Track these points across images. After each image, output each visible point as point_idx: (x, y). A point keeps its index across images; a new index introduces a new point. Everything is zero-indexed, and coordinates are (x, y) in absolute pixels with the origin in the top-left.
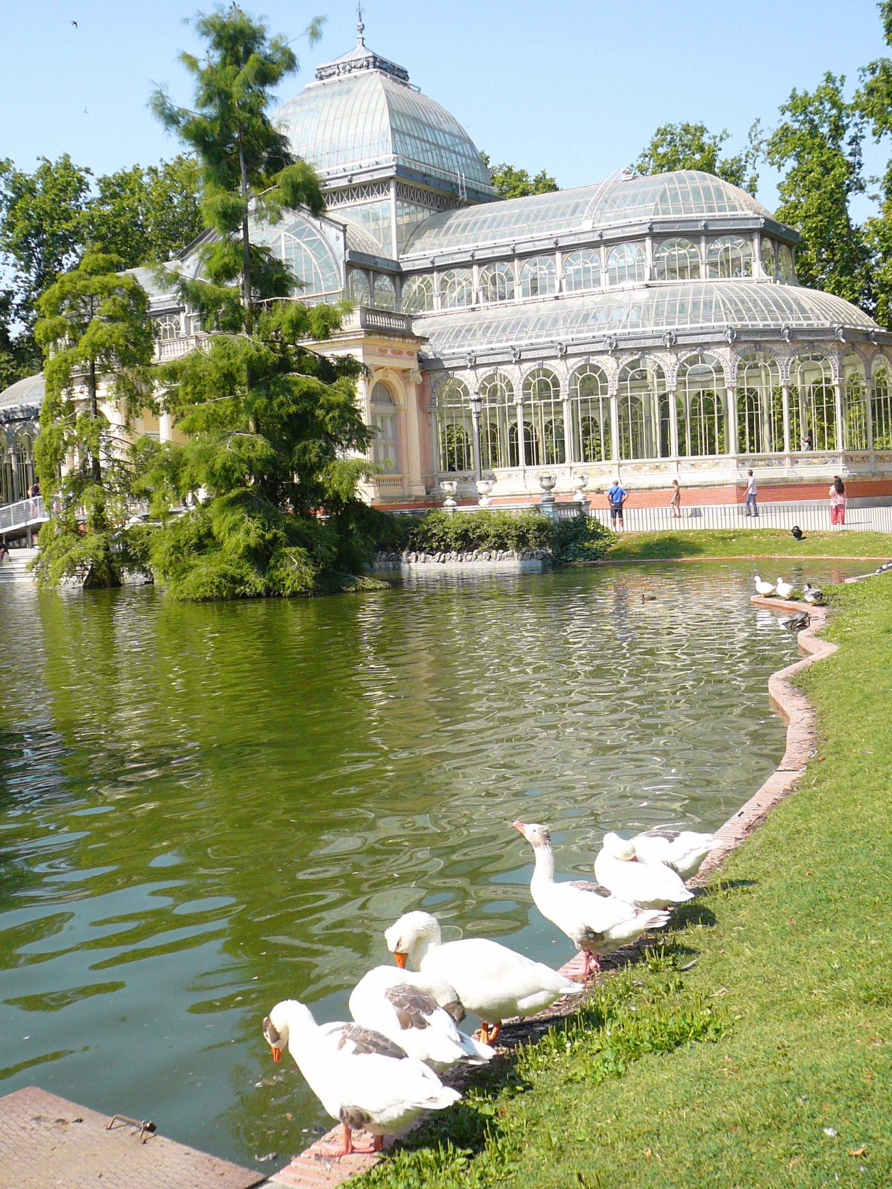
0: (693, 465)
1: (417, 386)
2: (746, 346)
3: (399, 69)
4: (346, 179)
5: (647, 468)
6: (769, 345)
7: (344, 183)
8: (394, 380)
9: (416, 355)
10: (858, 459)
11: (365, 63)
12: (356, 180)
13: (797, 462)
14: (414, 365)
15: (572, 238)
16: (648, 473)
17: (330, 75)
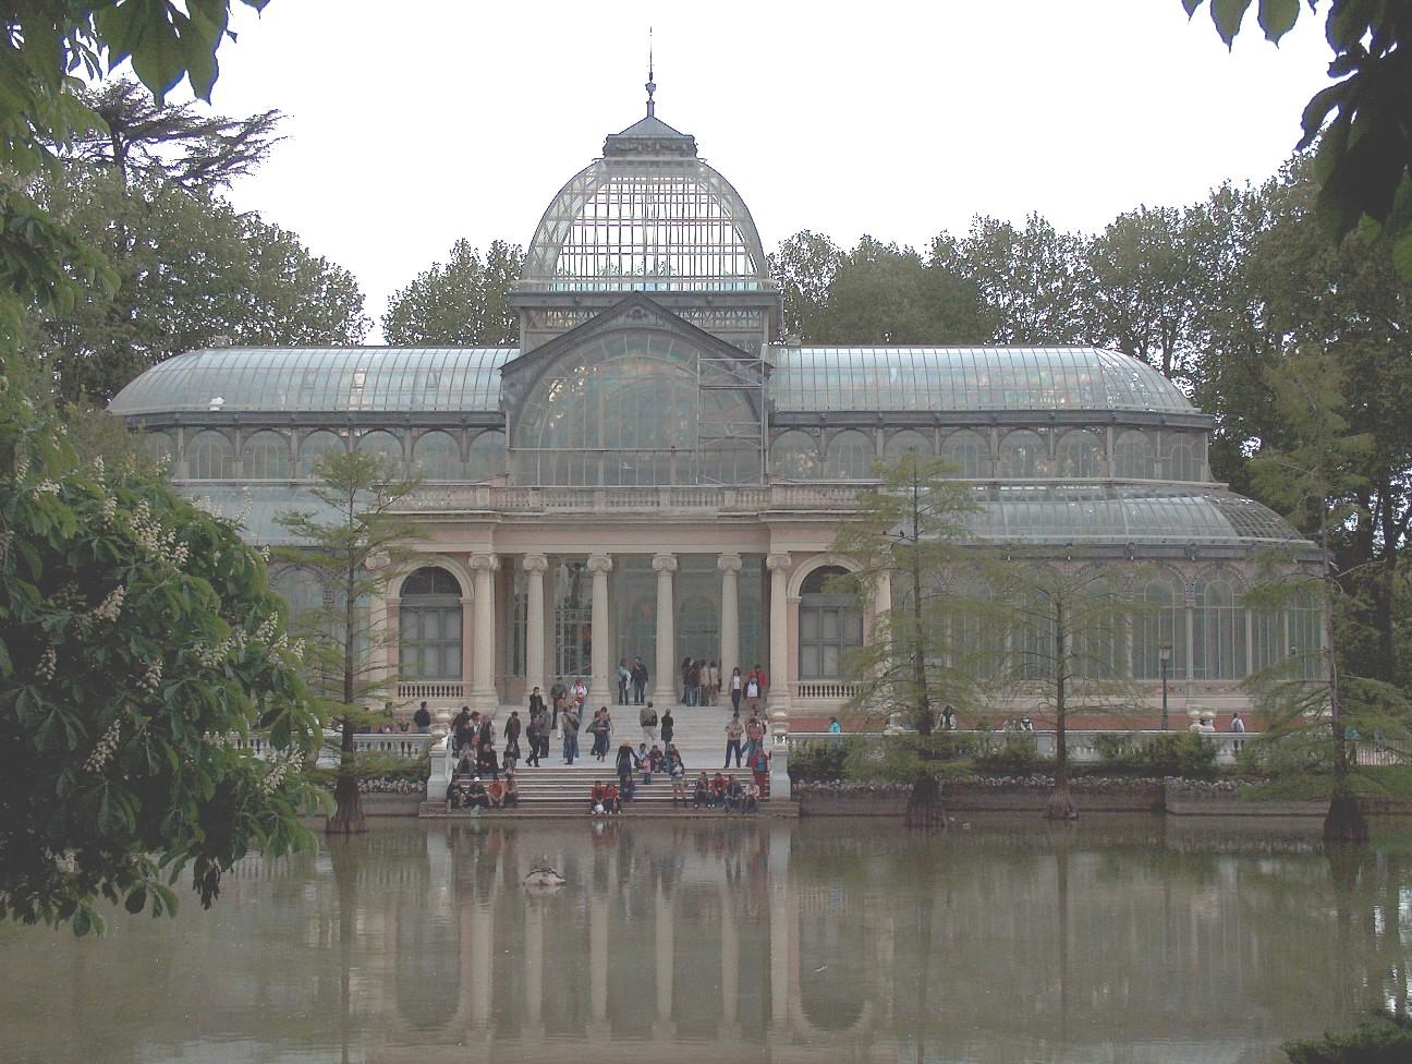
0: (1209, 689)
17: (630, 150)
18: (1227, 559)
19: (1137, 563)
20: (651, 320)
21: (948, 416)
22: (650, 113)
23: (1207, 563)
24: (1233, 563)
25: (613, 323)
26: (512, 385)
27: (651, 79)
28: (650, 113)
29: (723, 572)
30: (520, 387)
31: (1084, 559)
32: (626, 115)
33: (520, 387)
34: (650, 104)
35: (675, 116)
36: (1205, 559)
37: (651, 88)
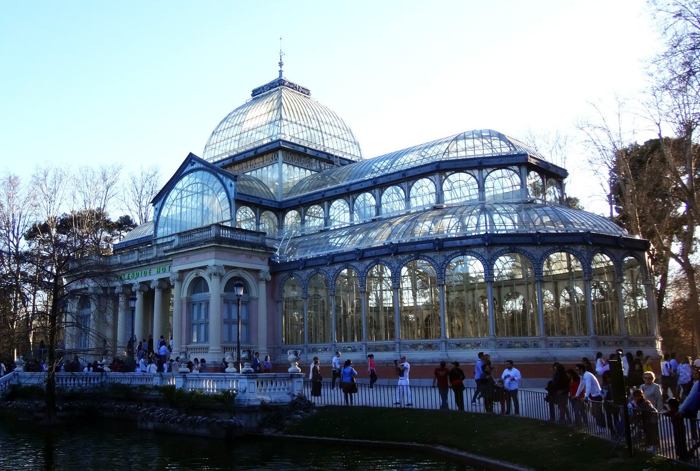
1: (267, 282)
2: (502, 248)
3: (303, 89)
4: (253, 152)
5: (422, 347)
6: (522, 248)
7: (252, 154)
8: (248, 278)
9: (267, 261)
10: (610, 343)
11: (278, 84)
12: (259, 151)
13: (551, 345)
14: (265, 268)
15: (385, 178)
16: (423, 351)
18: (468, 246)
19: (400, 257)
22: (281, 75)
23: (454, 252)
24: (475, 250)
27: (281, 59)
28: (281, 75)
31: (369, 258)
34: (281, 72)
36: (451, 248)
37: (281, 64)
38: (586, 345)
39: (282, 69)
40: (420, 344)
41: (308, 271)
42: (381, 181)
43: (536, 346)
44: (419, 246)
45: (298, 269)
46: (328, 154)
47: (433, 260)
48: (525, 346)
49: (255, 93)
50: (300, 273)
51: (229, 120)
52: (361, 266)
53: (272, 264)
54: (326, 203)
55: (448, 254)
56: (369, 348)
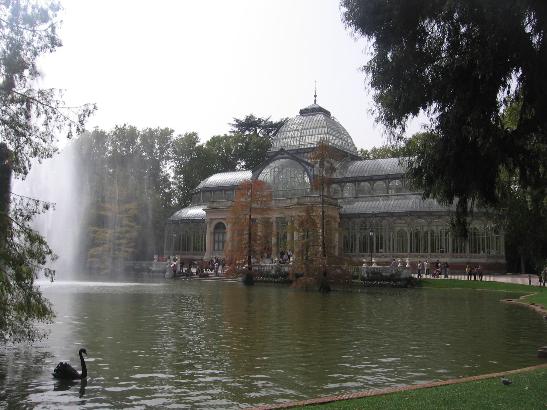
11: (318, 110)
13: (471, 257)
14: (338, 216)
18: (442, 215)
19: (411, 217)
20: (286, 155)
21: (374, 177)
22: (315, 102)
23: (436, 217)
24: (445, 217)
25: (277, 157)
26: (255, 175)
28: (315, 102)
29: (287, 222)
30: (256, 175)
31: (395, 216)
32: (308, 103)
33: (256, 175)
34: (315, 101)
35: (321, 104)
36: (435, 215)
37: (315, 96)
38: (484, 258)
39: (316, 99)
40: (419, 255)
41: (360, 219)
42: (390, 177)
43: (466, 257)
44: (422, 214)
45: (356, 218)
46: (346, 152)
47: (426, 220)
48: (462, 257)
49: (303, 112)
50: (356, 219)
51: (290, 127)
52: (391, 220)
53: (340, 214)
54: (357, 183)
55: (433, 218)
56: (394, 256)
